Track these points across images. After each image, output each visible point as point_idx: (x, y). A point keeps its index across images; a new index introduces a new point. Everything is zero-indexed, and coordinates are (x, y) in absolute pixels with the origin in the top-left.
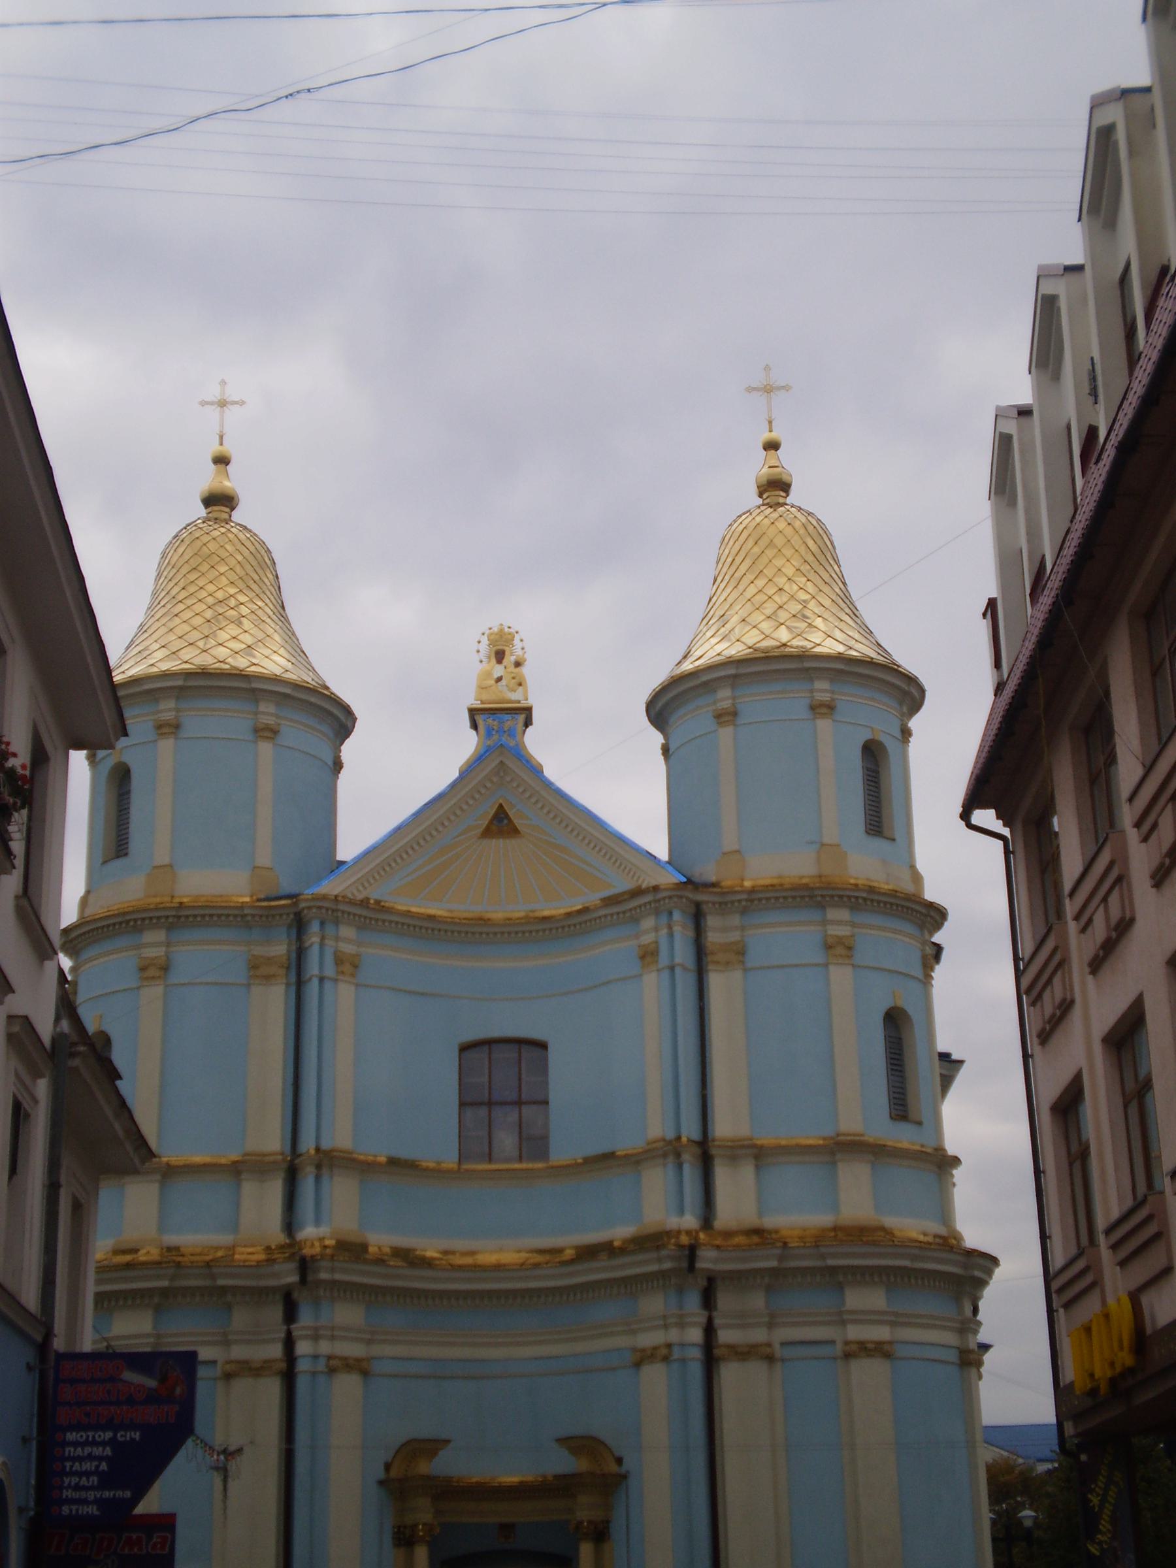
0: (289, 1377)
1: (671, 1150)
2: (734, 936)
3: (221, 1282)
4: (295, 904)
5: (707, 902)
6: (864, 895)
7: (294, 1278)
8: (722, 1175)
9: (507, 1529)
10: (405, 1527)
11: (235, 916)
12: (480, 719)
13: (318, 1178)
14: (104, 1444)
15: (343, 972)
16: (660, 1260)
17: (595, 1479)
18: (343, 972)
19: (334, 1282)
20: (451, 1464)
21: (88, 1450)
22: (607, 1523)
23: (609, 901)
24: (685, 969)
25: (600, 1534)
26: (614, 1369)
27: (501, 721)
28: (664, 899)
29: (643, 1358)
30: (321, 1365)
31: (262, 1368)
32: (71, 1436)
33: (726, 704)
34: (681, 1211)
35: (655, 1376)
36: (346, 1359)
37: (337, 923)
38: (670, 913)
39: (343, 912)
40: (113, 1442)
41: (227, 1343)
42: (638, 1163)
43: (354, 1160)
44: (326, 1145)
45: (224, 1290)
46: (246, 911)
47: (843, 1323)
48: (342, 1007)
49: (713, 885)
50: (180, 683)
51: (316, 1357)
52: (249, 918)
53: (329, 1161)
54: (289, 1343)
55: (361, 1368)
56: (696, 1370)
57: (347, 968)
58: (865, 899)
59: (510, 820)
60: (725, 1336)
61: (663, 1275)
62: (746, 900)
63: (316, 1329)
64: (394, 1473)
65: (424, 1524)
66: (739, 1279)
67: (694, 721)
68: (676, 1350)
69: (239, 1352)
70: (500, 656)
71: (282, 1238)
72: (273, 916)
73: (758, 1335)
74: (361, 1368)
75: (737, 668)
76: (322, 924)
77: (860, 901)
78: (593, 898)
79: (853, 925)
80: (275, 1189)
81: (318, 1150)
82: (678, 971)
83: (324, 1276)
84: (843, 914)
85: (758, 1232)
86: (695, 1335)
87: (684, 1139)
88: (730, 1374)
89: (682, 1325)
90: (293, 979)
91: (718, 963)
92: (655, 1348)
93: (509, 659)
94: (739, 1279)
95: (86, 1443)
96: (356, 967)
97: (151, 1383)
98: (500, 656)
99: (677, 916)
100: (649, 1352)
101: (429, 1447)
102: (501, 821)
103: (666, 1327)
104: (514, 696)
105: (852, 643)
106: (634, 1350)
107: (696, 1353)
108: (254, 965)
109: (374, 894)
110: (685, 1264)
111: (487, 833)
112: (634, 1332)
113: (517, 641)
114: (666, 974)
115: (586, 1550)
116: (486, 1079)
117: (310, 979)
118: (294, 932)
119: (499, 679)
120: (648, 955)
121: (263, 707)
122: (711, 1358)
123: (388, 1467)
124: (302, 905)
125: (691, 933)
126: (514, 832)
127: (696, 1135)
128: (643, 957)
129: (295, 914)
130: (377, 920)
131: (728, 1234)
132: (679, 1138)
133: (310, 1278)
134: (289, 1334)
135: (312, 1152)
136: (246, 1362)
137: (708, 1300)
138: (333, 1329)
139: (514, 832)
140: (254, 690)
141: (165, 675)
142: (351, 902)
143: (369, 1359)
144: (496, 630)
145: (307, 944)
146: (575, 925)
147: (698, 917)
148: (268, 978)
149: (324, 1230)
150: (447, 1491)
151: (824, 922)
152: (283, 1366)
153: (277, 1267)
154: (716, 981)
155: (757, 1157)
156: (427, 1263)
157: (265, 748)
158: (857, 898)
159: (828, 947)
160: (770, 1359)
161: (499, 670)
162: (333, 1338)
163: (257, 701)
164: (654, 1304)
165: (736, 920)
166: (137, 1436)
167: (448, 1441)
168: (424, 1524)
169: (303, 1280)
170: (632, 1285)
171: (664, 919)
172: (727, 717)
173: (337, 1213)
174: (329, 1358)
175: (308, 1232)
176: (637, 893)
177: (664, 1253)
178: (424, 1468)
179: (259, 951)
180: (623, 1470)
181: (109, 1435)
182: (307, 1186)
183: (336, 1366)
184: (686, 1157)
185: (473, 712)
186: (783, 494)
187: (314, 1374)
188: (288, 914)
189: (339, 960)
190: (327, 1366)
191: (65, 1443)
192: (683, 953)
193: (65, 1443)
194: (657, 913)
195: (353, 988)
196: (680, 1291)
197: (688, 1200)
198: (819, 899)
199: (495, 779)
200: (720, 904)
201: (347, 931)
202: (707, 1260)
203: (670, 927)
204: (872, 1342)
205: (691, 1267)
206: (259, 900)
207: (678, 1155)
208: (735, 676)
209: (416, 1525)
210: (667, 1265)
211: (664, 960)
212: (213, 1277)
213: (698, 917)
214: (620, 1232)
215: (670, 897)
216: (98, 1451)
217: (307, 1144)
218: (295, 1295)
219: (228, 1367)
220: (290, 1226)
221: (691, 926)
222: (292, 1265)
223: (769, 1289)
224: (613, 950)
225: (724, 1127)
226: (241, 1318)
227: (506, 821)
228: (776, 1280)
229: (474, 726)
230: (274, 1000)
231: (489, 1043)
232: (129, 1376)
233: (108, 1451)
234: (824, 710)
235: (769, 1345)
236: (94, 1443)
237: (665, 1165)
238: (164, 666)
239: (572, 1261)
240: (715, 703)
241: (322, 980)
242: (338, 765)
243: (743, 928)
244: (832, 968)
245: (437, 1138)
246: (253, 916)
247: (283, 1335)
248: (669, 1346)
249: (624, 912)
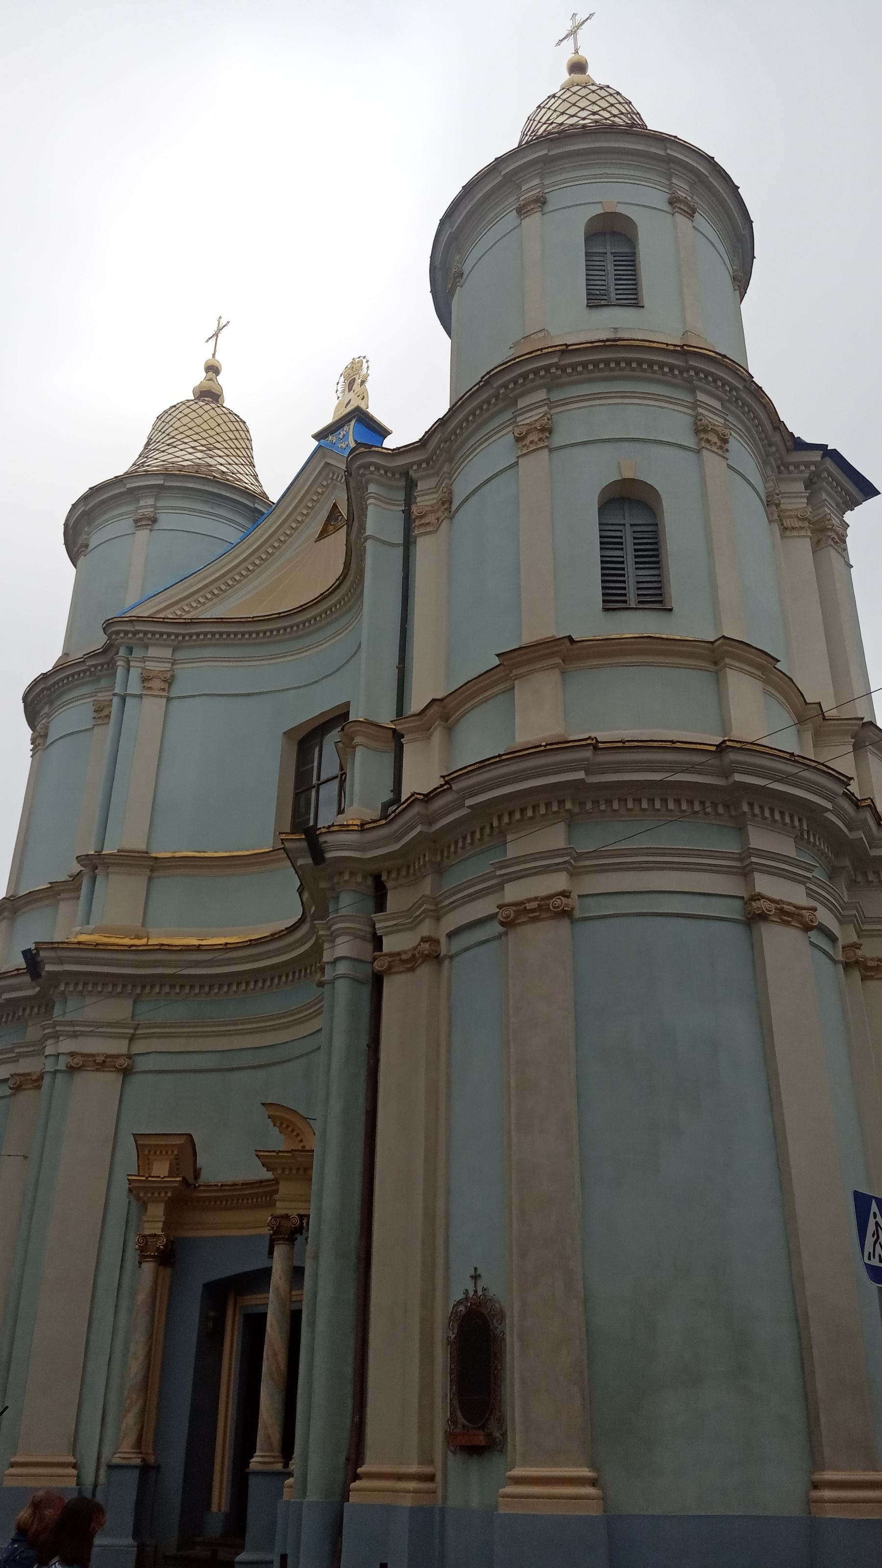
39: (145, 633)
46: (89, 663)
57: (156, 684)
138: (72, 1023)
154: (424, 548)
162: (75, 1035)
246: (95, 666)
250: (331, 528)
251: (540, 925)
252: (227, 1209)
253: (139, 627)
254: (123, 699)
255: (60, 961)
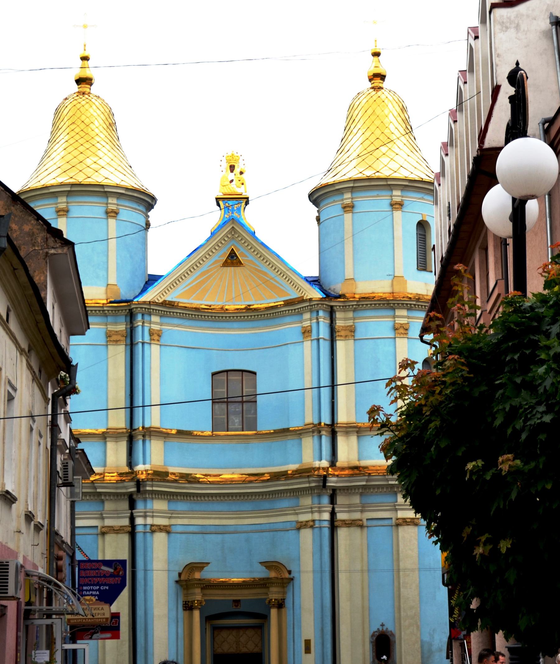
0: (132, 534)
1: (316, 429)
2: (350, 323)
3: (98, 490)
4: (130, 306)
5: (336, 306)
6: (414, 303)
7: (134, 489)
8: (341, 441)
9: (237, 602)
10: (188, 602)
11: (99, 311)
12: (221, 203)
13: (144, 441)
14: (96, 590)
15: (154, 340)
16: (309, 482)
17: (278, 580)
18: (154, 340)
19: (153, 492)
20: (211, 574)
21: (91, 592)
22: (283, 600)
23: (288, 303)
24: (324, 339)
25: (280, 605)
26: (288, 530)
27: (232, 202)
28: (315, 305)
29: (301, 526)
30: (148, 529)
31: (119, 530)
32: (85, 588)
33: (348, 201)
34: (321, 459)
35: (307, 535)
36: (159, 526)
37: (150, 315)
38: (318, 312)
39: (153, 309)
40: (99, 590)
41: (103, 518)
42: (300, 434)
43: (161, 432)
44: (147, 425)
45: (100, 494)
46: (105, 309)
47: (396, 510)
48: (153, 357)
49: (340, 296)
50: (69, 189)
51: (145, 525)
52: (106, 312)
53: (150, 433)
54: (132, 519)
55: (167, 530)
56: (326, 532)
57: (156, 337)
58: (415, 305)
59: (237, 257)
60: (340, 516)
61: (311, 488)
62: (356, 305)
63: (145, 512)
64: (183, 577)
65: (197, 601)
66: (347, 490)
67: (332, 209)
68: (317, 523)
69: (108, 522)
70: (232, 168)
71: (127, 470)
72: (118, 311)
73: (356, 516)
74: (167, 530)
75: (354, 183)
76: (143, 315)
77: (412, 306)
78: (278, 300)
79: (408, 317)
80: (123, 446)
81: (143, 427)
82: (321, 341)
83: (148, 488)
84: (404, 312)
85: (357, 468)
86: (326, 516)
87: (323, 424)
88: (342, 534)
89: (320, 512)
90: (129, 342)
91: (341, 336)
92: (307, 522)
93: (237, 170)
94: (347, 490)
95: (89, 591)
96: (159, 336)
97: (111, 570)
98: (232, 168)
99: (321, 313)
100: (304, 523)
101: (199, 566)
102: (232, 257)
103: (312, 512)
104: (239, 191)
105: (412, 169)
106: (297, 522)
107: (326, 524)
108: (108, 335)
109: (169, 298)
110: (321, 484)
111: (226, 264)
112: (297, 514)
113: (241, 161)
114: (315, 342)
115: (274, 612)
116: (225, 390)
117: (137, 343)
118: (128, 319)
119: (232, 181)
120: (306, 332)
121: (110, 200)
122: (333, 526)
123: (180, 575)
124: (133, 306)
125: (328, 322)
126: (239, 264)
127: (328, 422)
128: (304, 333)
129: (129, 310)
130: (170, 312)
131: (343, 469)
132: (320, 423)
133: (142, 489)
134: (132, 514)
135: (141, 428)
136: (112, 527)
137: (333, 501)
139: (239, 264)
140: (106, 192)
141: (62, 185)
142: (157, 304)
143: (170, 526)
144: (230, 154)
145: (136, 325)
146: (270, 314)
147: (332, 313)
148: (116, 342)
149: (148, 467)
150: (208, 586)
151: (394, 317)
152: (130, 529)
153: (126, 484)
154: (340, 345)
155: (357, 432)
156: (196, 481)
157: (112, 222)
158: (411, 304)
159: (395, 329)
160: (361, 526)
161: (231, 176)
162: (153, 517)
163: (107, 198)
164: (307, 501)
165: (350, 314)
166: (107, 588)
167: (209, 563)
168: (197, 601)
169: (138, 491)
170: (297, 493)
171: (315, 315)
172: (349, 208)
173: (155, 456)
174: (152, 525)
175: (140, 467)
176: (301, 300)
177: (311, 479)
178: (197, 575)
179: (110, 328)
180: (291, 576)
181: (98, 587)
182: (139, 445)
183: (154, 529)
184: (323, 433)
185: (217, 200)
186: (382, 81)
187: (145, 533)
188: (126, 310)
189: (151, 333)
190: (150, 529)
191: (83, 590)
192: (324, 332)
193: (83, 590)
194: (311, 311)
195: (159, 346)
196: (319, 496)
197: (324, 453)
198: (392, 305)
199: (229, 236)
200: (343, 306)
201: (155, 319)
202: (332, 482)
203: (317, 319)
204: (409, 518)
205: (324, 486)
206: (111, 302)
207: (320, 432)
208: (353, 187)
209: (194, 601)
210: (313, 485)
211: (314, 336)
212: (95, 488)
213: (332, 313)
214: (292, 467)
215: (318, 304)
216: (94, 593)
217: (138, 424)
218: (135, 497)
219: (104, 530)
220: (131, 463)
221: (329, 319)
222: (133, 484)
223: (361, 494)
224: (289, 329)
225: (342, 418)
226: (109, 506)
227: (235, 258)
228: (365, 490)
229: (218, 205)
230: (119, 353)
231: (227, 371)
232: (104, 568)
233: (98, 593)
234: (397, 206)
235: (361, 520)
236: (93, 590)
237: (313, 436)
238: (60, 180)
239: (268, 480)
240: (343, 200)
241: (143, 343)
242: (148, 225)
243: (354, 319)
244: (397, 339)
245: (201, 419)
246: (108, 311)
247: (129, 515)
248: (314, 521)
249: (295, 310)
250: (229, 261)
251: (410, 527)
252: (216, 589)
253: (152, 307)
254: (143, 343)
255: (152, 486)
